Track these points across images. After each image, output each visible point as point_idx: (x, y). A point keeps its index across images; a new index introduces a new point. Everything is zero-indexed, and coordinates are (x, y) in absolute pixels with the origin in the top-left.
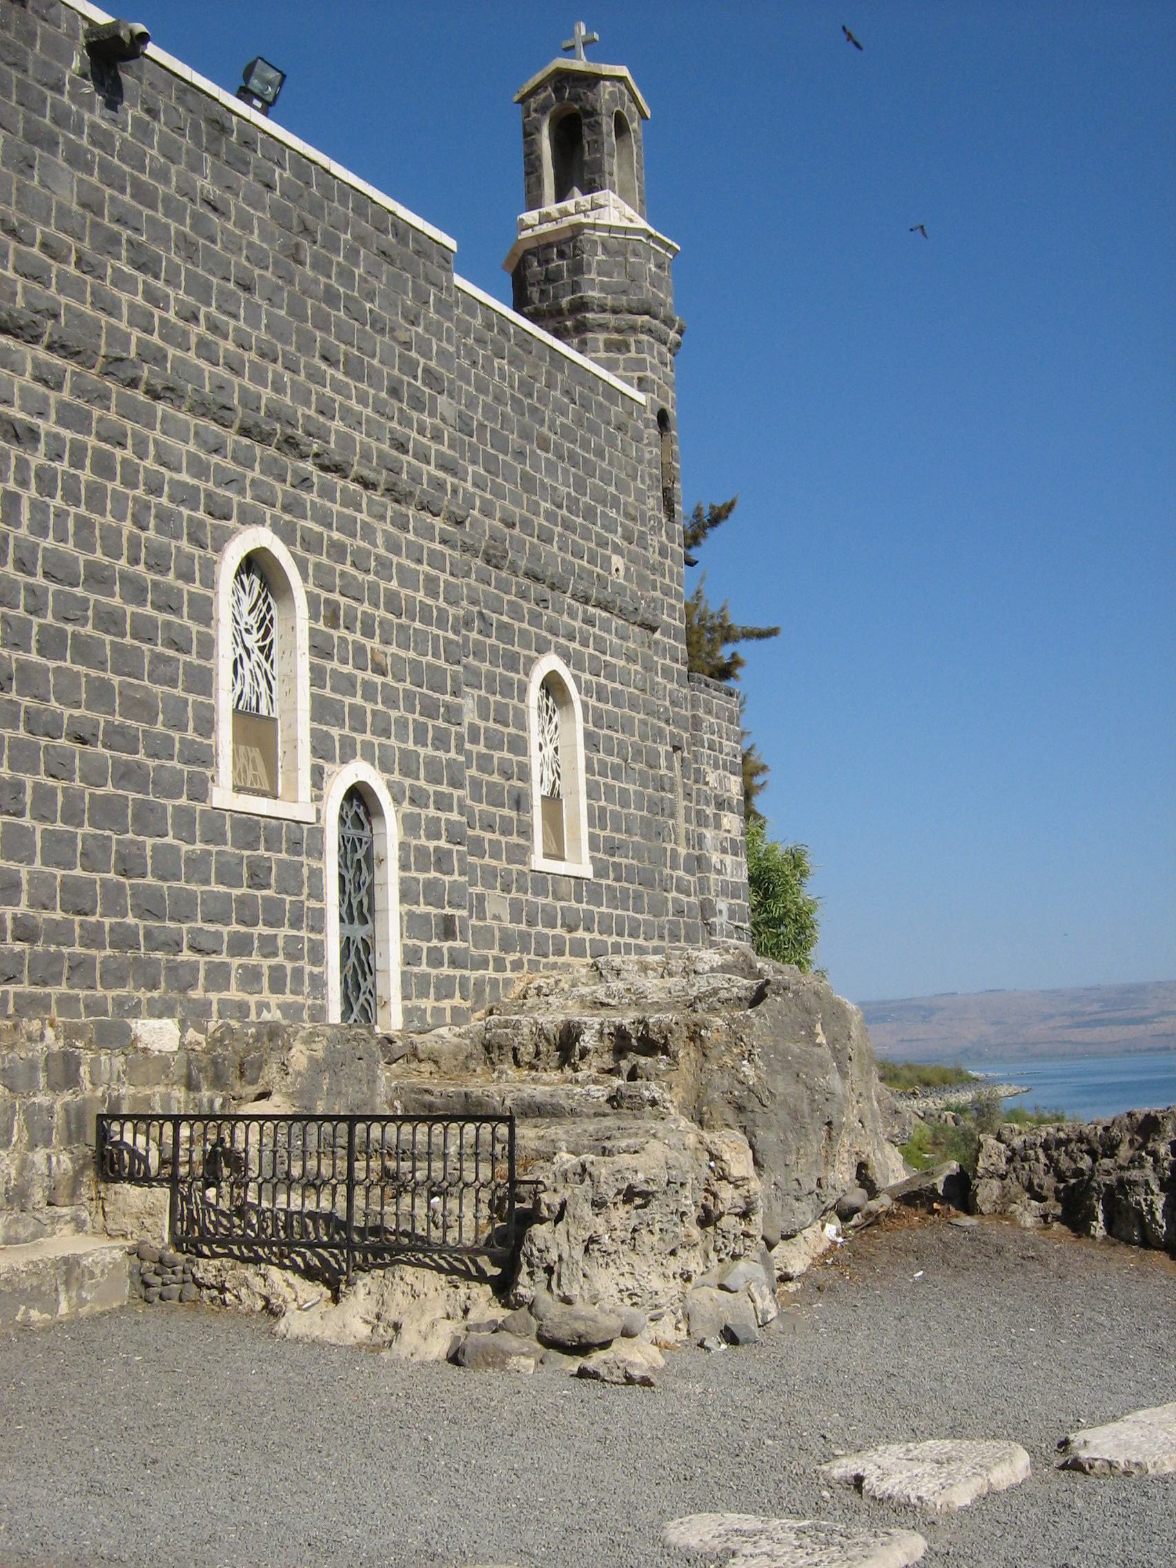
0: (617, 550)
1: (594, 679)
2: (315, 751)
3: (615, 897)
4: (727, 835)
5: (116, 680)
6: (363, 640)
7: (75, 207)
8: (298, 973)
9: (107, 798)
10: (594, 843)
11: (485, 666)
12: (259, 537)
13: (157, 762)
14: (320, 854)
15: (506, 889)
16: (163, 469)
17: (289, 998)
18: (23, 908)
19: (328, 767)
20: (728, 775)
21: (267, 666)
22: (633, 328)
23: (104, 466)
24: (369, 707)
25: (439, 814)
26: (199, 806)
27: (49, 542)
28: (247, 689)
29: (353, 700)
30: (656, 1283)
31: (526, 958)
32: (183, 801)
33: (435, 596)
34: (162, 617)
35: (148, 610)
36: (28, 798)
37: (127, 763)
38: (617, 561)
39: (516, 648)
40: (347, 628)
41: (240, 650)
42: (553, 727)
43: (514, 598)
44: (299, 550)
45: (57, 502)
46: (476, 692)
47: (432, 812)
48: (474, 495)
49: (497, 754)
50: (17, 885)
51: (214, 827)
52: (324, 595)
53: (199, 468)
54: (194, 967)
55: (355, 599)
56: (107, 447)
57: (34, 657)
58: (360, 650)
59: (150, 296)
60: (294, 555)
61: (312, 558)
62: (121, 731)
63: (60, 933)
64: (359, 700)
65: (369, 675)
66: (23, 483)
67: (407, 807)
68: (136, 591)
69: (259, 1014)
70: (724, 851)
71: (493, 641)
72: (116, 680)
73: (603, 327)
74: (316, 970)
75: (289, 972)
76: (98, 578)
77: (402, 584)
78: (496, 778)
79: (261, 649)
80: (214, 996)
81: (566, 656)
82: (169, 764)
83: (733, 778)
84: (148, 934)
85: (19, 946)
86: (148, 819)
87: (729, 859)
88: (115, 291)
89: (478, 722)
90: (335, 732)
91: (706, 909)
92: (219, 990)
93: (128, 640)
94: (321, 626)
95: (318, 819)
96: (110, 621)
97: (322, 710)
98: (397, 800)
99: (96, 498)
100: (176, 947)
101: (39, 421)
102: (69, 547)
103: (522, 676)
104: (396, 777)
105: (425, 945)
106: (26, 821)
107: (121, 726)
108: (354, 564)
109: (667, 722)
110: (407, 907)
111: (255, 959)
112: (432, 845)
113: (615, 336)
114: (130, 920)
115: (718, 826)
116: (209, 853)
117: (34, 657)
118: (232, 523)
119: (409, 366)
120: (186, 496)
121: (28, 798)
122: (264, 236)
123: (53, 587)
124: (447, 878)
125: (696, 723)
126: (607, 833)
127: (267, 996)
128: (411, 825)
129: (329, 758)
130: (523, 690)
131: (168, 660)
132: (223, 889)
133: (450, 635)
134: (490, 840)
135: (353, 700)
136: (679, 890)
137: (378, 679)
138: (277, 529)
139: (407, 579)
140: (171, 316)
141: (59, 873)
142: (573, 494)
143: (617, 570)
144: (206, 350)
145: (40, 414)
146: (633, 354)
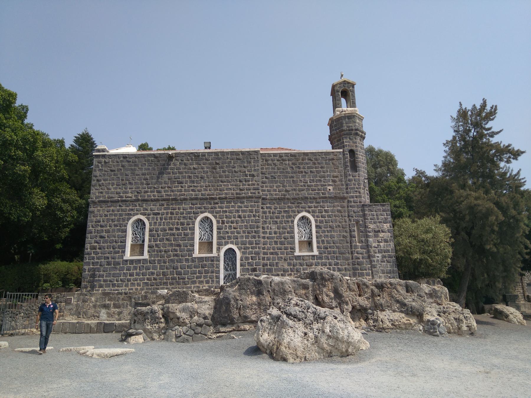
0: (329, 185)
1: (320, 214)
2: (218, 245)
3: (328, 258)
5: (173, 242)
6: (231, 224)
7: (167, 180)
8: (213, 281)
9: (171, 259)
10: (318, 247)
11: (278, 220)
12: (206, 214)
13: (181, 252)
14: (219, 261)
15: (285, 260)
16: (184, 211)
17: (210, 285)
18: (155, 276)
19: (221, 247)
20: (383, 224)
21: (212, 233)
22: (341, 136)
23: (172, 213)
24: (232, 235)
25: (252, 250)
26: (190, 257)
27: (162, 227)
28: (206, 237)
29: (228, 235)
30: (149, 327)
31: (293, 273)
32: (187, 257)
33: (253, 212)
34: (183, 232)
35: (181, 231)
36: (156, 262)
37: (175, 254)
38: (331, 188)
39: (291, 214)
40: (227, 223)
41: (205, 232)
42: (309, 226)
43: (290, 205)
44: (215, 214)
45: (164, 221)
46: (276, 225)
47: (250, 250)
48: (276, 189)
49: (283, 235)
50: (154, 273)
51: (193, 260)
52: (221, 220)
53: (191, 208)
54: (188, 282)
55: (229, 218)
56: (173, 211)
57: (159, 242)
58: (231, 226)
59: (182, 187)
60: (213, 216)
61: (218, 215)
62: (175, 249)
63: (160, 279)
64: (230, 235)
65: (233, 230)
66: (157, 220)
67: (243, 250)
68: (178, 229)
69: (202, 288)
70: (379, 242)
71: (283, 214)
72: (173, 242)
73: (335, 138)
74: (217, 280)
75: (210, 281)
76: (171, 229)
77: (242, 212)
78: (283, 239)
79: (210, 231)
80: (193, 286)
81: (309, 212)
82: (184, 252)
83: (385, 225)
84: (178, 277)
85: (154, 281)
86: (180, 261)
87: (381, 244)
88: (175, 189)
89: (277, 230)
90: (223, 241)
91: (369, 257)
92: (194, 284)
93: (176, 236)
94: (221, 224)
95: (218, 256)
96: (174, 235)
97: (219, 238)
98: (239, 249)
99: (171, 218)
100: (184, 279)
101: (160, 211)
102: (166, 226)
103: (293, 219)
104: (240, 245)
105: (247, 274)
106: (156, 264)
107: (174, 249)
108: (229, 213)
109: (352, 217)
110: (242, 267)
111: (202, 279)
112: (250, 256)
113: (338, 139)
114: (175, 276)
115: (376, 236)
116: (192, 264)
117: (159, 242)
118: (199, 214)
119: (246, 176)
120: (190, 213)
121: (156, 262)
122: (207, 168)
123: (162, 232)
124: (254, 261)
125: (364, 215)
126: (325, 244)
127: (205, 284)
128: (243, 253)
129: (222, 245)
130: (293, 222)
131: (184, 237)
132: (195, 269)
133: (257, 218)
134: (280, 252)
135: (228, 235)
136: (357, 253)
137: (235, 230)
138: (209, 212)
139: (243, 211)
140: (186, 188)
141: (162, 270)
142: (312, 179)
143: (330, 190)
144: (193, 190)
145: (161, 210)
146: (342, 141)
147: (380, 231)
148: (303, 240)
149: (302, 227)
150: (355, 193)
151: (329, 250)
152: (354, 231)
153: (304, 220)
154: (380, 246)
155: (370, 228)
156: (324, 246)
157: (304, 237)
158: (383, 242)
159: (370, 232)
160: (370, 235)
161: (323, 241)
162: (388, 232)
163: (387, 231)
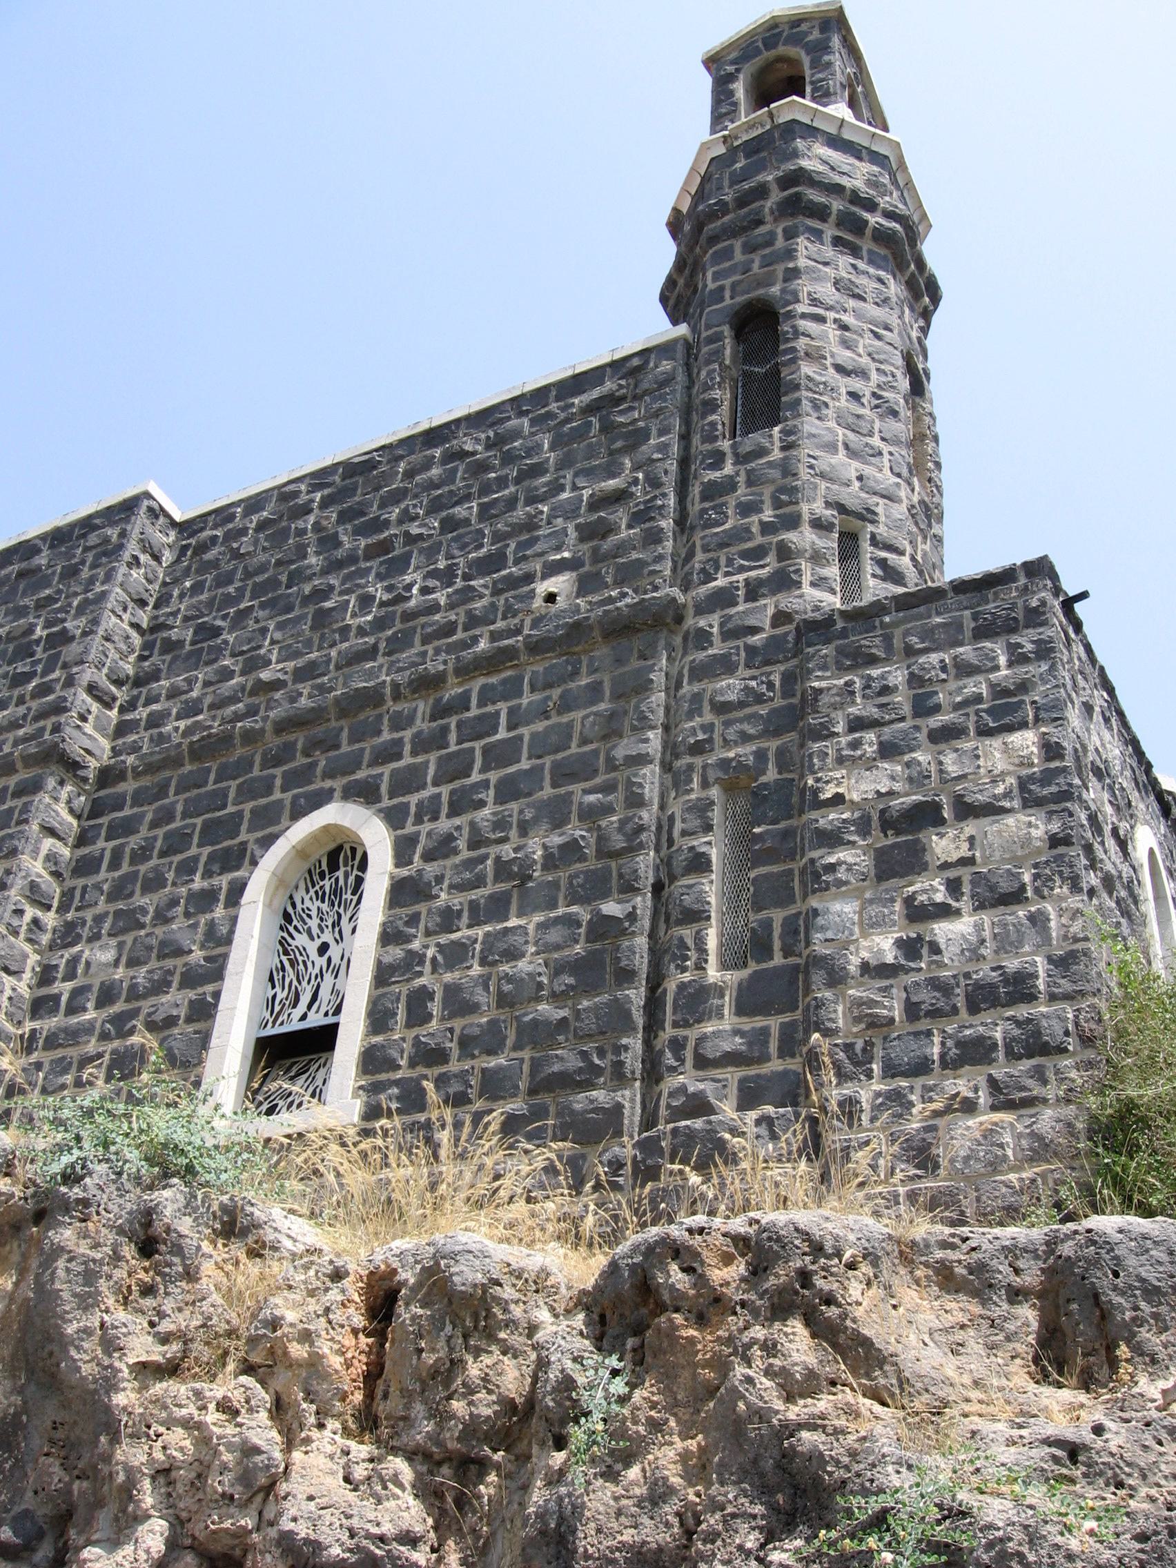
4: (965, 873)
38: (560, 584)
147: (937, 807)
148: (295, 1026)
149: (313, 923)
150: (742, 569)
151: (454, 1066)
152: (700, 864)
153: (340, 874)
154: (935, 949)
155: (838, 799)
156: (416, 1041)
157: (305, 999)
158: (965, 904)
159: (832, 839)
160: (832, 868)
161: (420, 998)
162: (1026, 804)
163: (1007, 795)
